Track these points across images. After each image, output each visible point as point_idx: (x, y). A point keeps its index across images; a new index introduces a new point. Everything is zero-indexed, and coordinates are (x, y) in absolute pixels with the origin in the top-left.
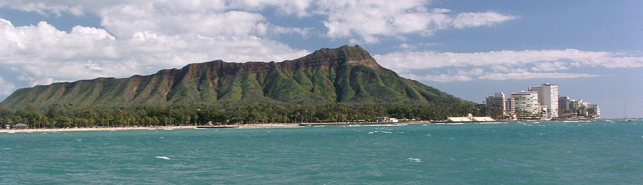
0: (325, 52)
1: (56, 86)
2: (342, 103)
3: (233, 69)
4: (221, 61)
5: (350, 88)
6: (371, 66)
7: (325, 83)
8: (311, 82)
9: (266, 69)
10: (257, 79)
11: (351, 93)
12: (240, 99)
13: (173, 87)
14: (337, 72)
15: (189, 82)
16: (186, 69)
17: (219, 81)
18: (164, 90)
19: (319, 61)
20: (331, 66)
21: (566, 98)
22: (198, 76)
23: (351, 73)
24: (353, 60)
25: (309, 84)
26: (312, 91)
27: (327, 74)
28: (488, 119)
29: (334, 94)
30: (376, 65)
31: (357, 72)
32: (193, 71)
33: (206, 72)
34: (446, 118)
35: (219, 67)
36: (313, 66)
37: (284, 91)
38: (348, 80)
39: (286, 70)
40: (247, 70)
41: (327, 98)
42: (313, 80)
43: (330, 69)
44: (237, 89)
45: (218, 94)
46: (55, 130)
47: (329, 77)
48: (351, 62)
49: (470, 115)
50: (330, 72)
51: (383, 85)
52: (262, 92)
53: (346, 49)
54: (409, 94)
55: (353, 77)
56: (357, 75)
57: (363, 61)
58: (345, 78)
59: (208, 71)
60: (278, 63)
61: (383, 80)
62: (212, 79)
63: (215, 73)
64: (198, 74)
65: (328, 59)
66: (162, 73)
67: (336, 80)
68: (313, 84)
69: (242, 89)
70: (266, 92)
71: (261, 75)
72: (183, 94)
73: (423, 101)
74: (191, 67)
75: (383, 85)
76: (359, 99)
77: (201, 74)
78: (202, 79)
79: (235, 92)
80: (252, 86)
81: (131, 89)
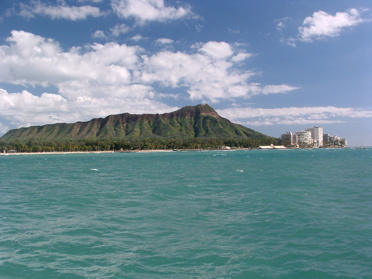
0: (188, 108)
1: (33, 128)
2: (198, 138)
3: (135, 118)
4: (128, 114)
5: (203, 129)
6: (214, 116)
7: (188, 126)
8: (180, 126)
9: (154, 118)
10: (149, 124)
11: (203, 132)
12: (139, 136)
13: (100, 128)
14: (195, 120)
15: (109, 125)
16: (108, 118)
17: (127, 125)
18: (95, 130)
19: (185, 114)
20: (191, 116)
21: (327, 135)
22: (114, 122)
23: (203, 120)
24: (204, 113)
25: (179, 127)
26: (181, 131)
27: (189, 121)
28: (283, 147)
29: (193, 133)
30: (217, 116)
31: (206, 120)
32: (111, 119)
33: (119, 119)
34: (258, 147)
35: (127, 117)
36: (181, 116)
37: (164, 131)
38: (201, 125)
39: (165, 119)
40: (143, 119)
41: (189, 135)
42: (181, 124)
43: (191, 118)
44: (137, 130)
45: (126, 132)
46: (32, 153)
47: (190, 123)
48: (203, 114)
49: (272, 145)
50: (191, 120)
51: (222, 127)
52: (151, 131)
53: (200, 107)
54: (237, 132)
55: (204, 122)
56: (206, 121)
57: (210, 113)
58: (200, 123)
59: (121, 119)
60: (161, 115)
61: (222, 124)
62: (123, 124)
63: (124, 121)
64: (115, 121)
65: (190, 112)
66: (94, 120)
67: (195, 124)
68: (181, 127)
69: (140, 129)
70: (154, 131)
71: (151, 121)
72: (106, 133)
73: (245, 136)
74: (110, 117)
75: (222, 127)
76: (208, 135)
77: (116, 121)
78: (117, 124)
79: (136, 131)
80: (146, 128)
81: (76, 129)
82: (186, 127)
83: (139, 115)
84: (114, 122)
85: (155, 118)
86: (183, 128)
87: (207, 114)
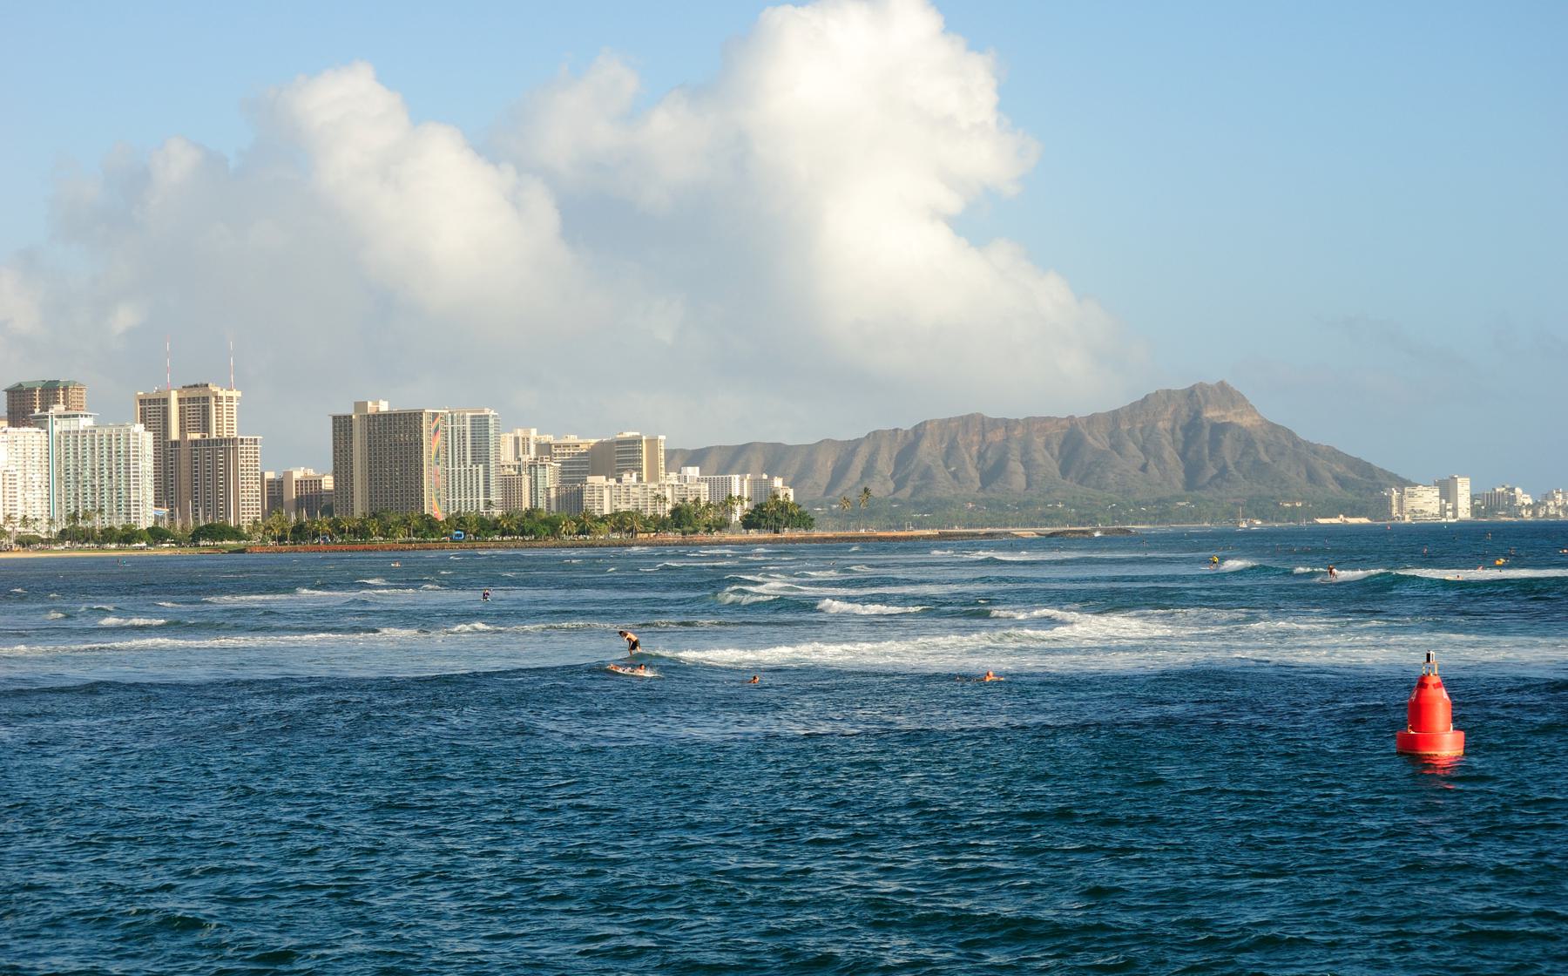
6: (1246, 421)
7: (1166, 455)
15: (928, 451)
18: (885, 465)
20: (1175, 421)
21: (1513, 490)
22: (941, 441)
26: (1144, 468)
29: (1182, 476)
42: (1143, 449)
43: (1173, 431)
54: (1312, 477)
61: (1267, 451)
65: (1171, 409)
70: (1065, 472)
73: (1333, 487)
75: (1266, 459)
80: (1041, 460)
82: (1160, 459)
84: (941, 441)
85: (1063, 427)
86: (1151, 462)
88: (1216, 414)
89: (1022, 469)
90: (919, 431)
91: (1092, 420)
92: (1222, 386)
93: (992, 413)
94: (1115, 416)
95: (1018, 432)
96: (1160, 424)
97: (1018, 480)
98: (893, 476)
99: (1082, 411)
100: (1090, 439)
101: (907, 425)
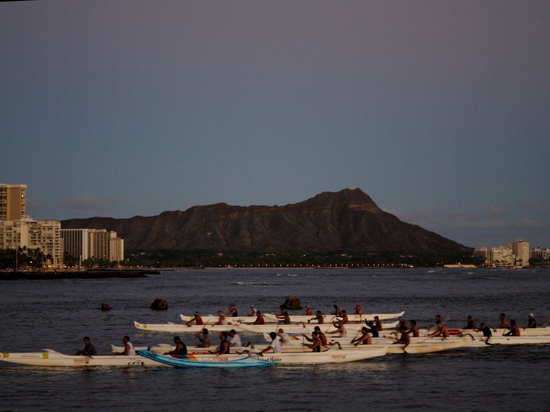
6: (372, 210)
26: (317, 235)
28: (473, 266)
30: (376, 209)
38: (352, 226)
49: (459, 263)
74: (195, 210)
83: (245, 207)
85: (271, 212)
87: (359, 208)
88: (355, 206)
89: (249, 234)
90: (191, 211)
91: (288, 207)
92: (358, 191)
93: (232, 203)
94: (299, 207)
95: (246, 214)
96: (325, 211)
97: (247, 241)
98: (176, 236)
99: (282, 203)
100: (286, 218)
101: (183, 209)
